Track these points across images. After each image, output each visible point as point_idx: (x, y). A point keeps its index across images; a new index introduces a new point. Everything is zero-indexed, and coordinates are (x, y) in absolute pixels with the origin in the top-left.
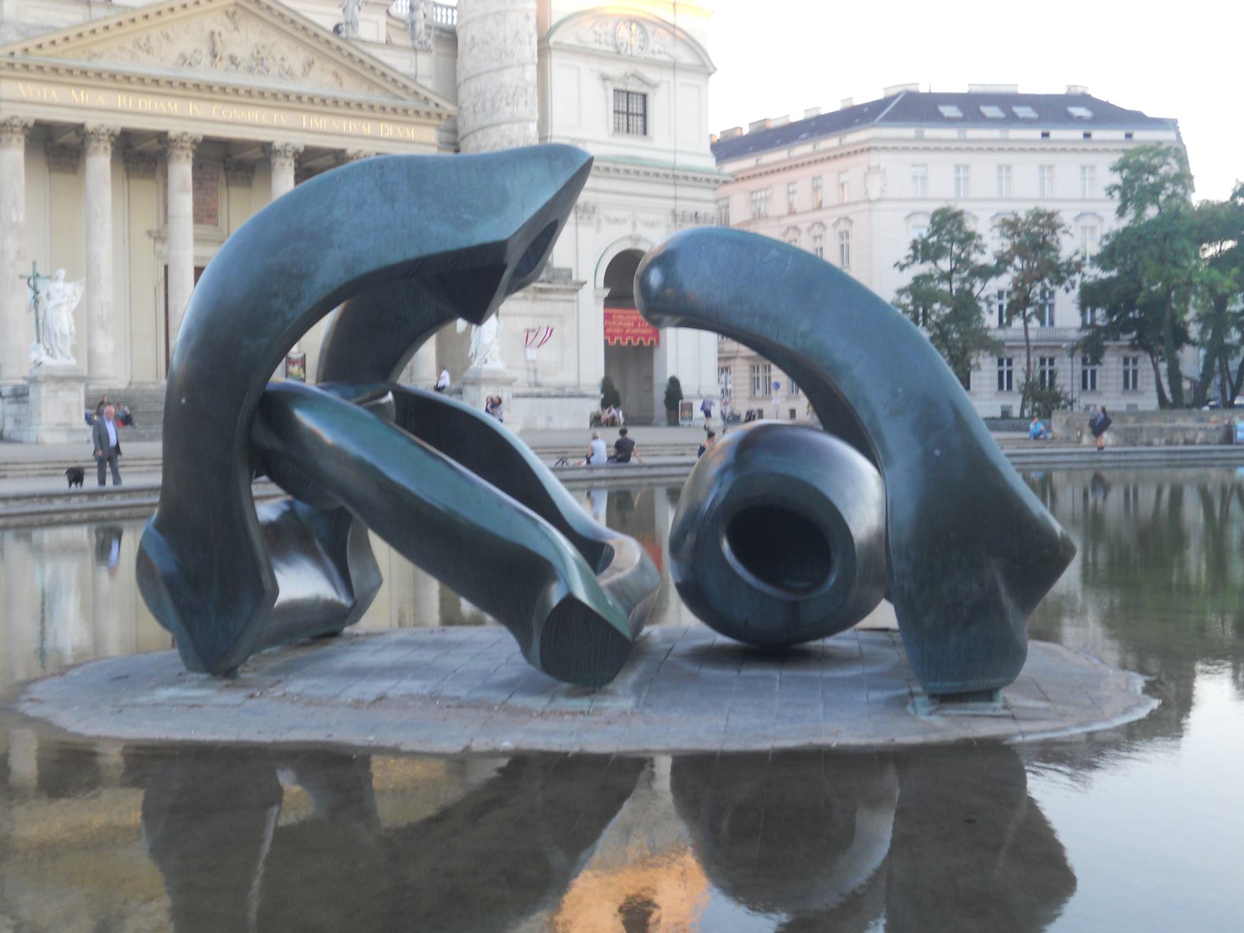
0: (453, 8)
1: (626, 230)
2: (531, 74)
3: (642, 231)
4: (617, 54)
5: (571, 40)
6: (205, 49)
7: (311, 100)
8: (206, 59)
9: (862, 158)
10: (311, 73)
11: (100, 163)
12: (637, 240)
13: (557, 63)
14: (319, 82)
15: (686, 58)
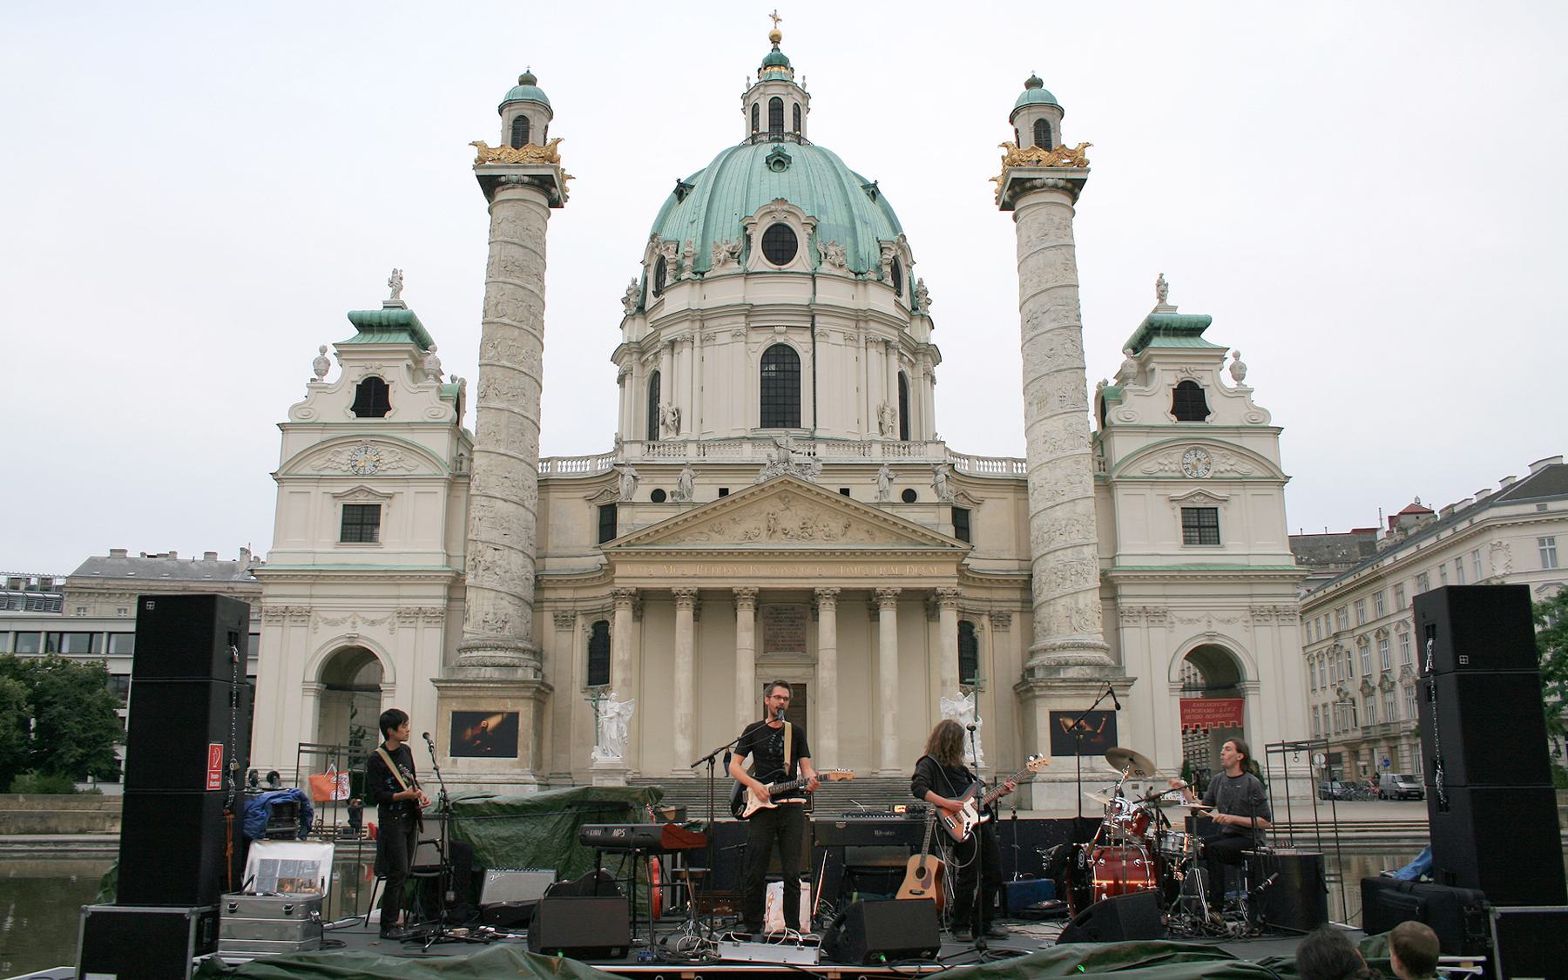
0: (1022, 461)
1: (1202, 628)
2: (1087, 508)
3: (1217, 628)
4: (1182, 480)
5: (1135, 471)
6: (763, 526)
7: (843, 553)
8: (764, 533)
9: (1487, 537)
10: (849, 534)
11: (684, 615)
12: (1212, 636)
13: (1120, 493)
14: (857, 540)
15: (1258, 472)
